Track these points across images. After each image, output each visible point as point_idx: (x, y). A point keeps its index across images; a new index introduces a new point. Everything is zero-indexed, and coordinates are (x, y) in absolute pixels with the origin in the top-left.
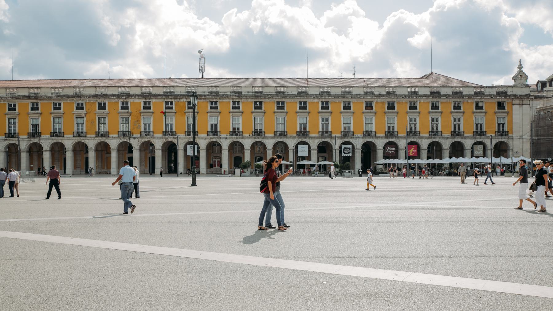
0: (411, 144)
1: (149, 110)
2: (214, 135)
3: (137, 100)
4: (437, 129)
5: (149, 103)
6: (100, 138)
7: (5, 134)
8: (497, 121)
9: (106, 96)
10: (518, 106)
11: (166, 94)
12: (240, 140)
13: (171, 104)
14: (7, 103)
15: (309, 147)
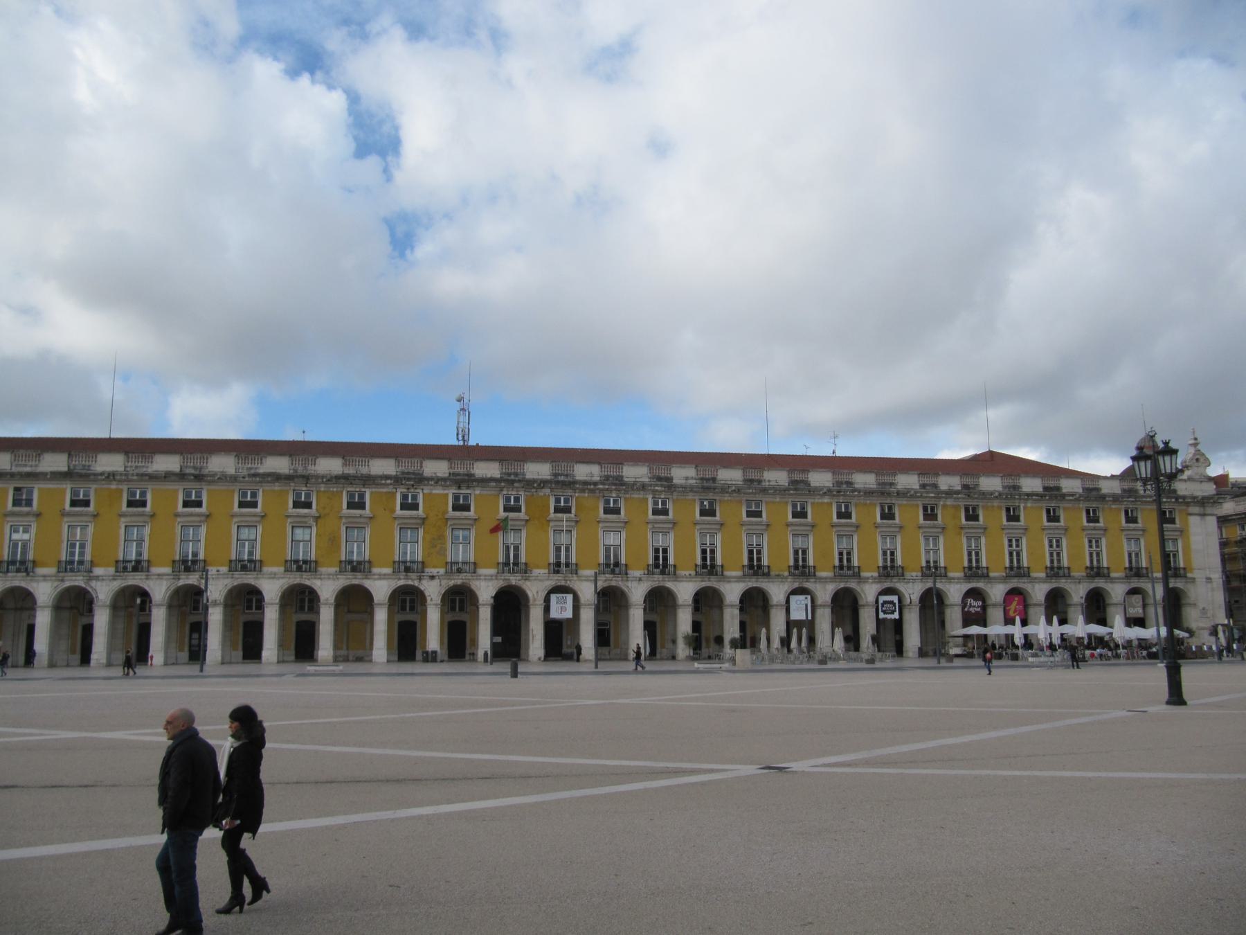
0: (1134, 591)
1: (466, 514)
2: (613, 572)
3: (438, 491)
4: (935, 562)
5: (466, 498)
6: (350, 575)
7: (117, 562)
8: (1126, 548)
9: (368, 480)
10: (1198, 518)
11: (506, 477)
12: (669, 585)
13: (517, 499)
14: (125, 487)
15: (576, 599)
